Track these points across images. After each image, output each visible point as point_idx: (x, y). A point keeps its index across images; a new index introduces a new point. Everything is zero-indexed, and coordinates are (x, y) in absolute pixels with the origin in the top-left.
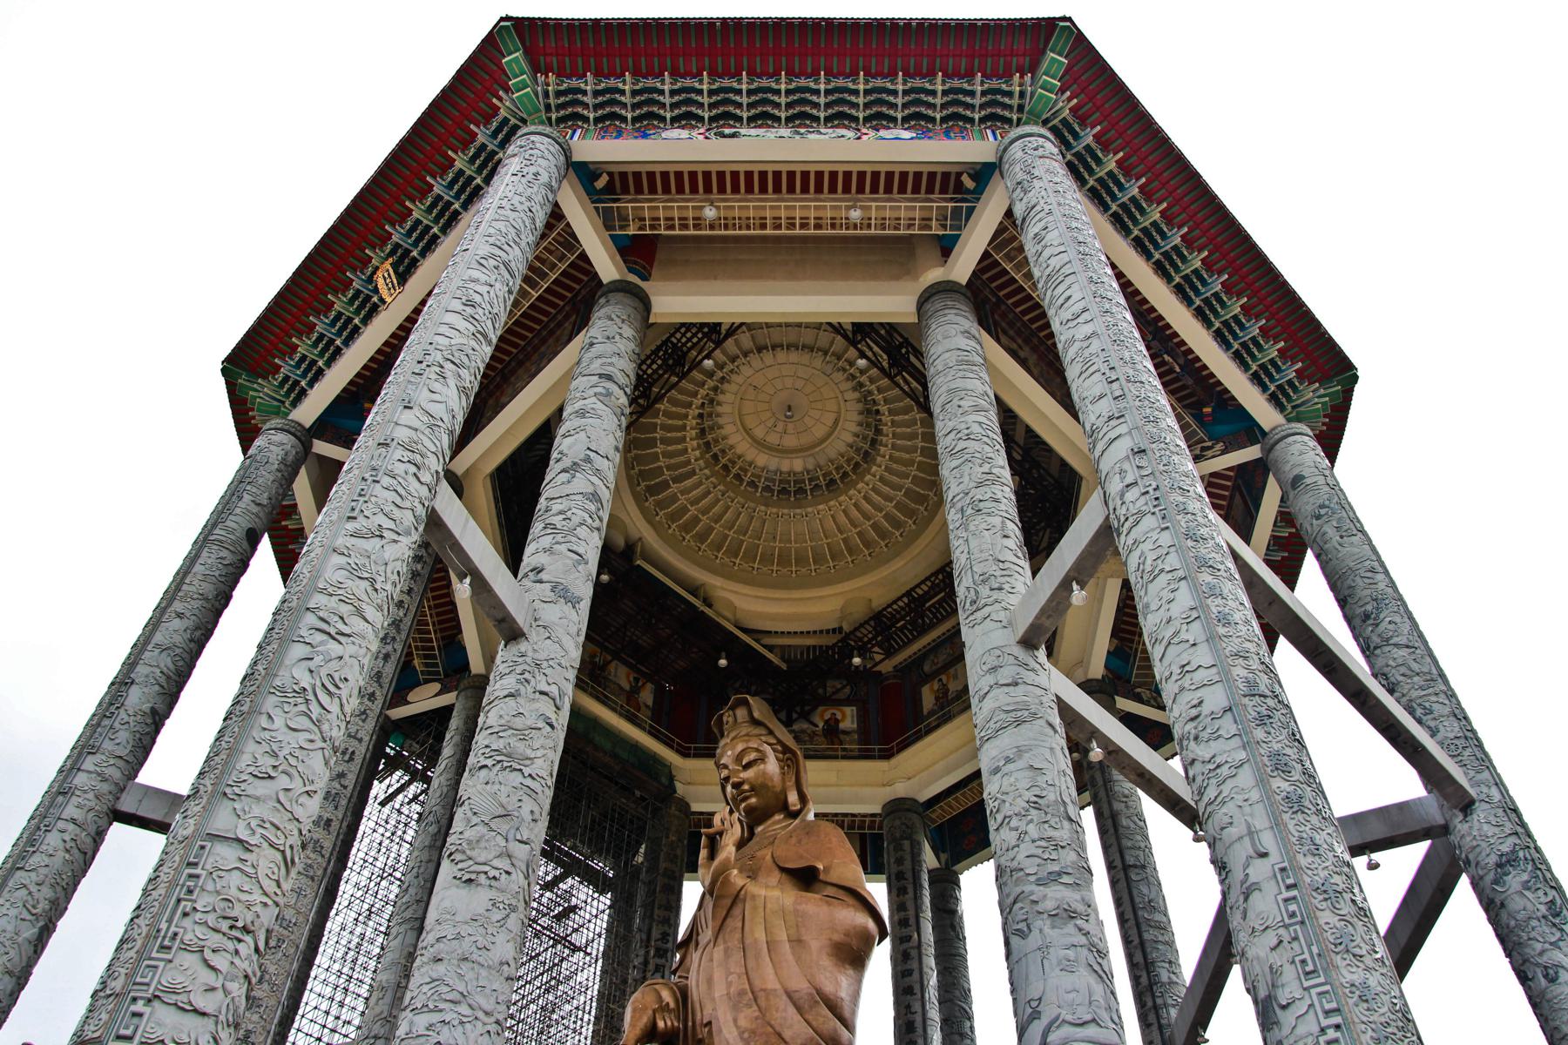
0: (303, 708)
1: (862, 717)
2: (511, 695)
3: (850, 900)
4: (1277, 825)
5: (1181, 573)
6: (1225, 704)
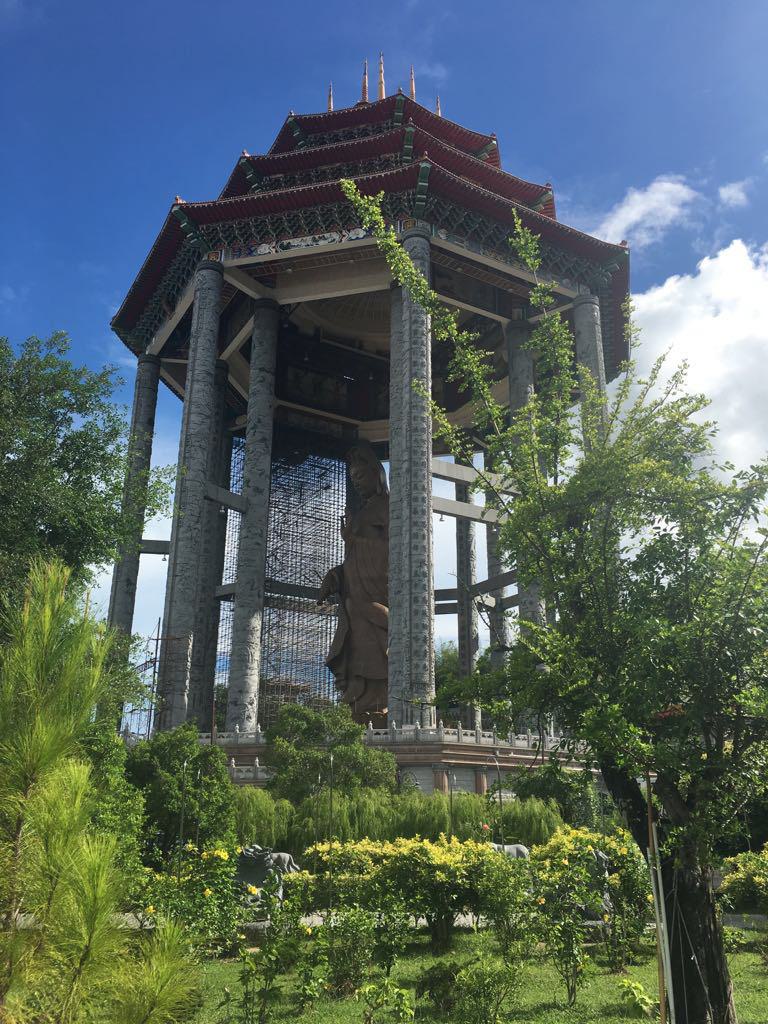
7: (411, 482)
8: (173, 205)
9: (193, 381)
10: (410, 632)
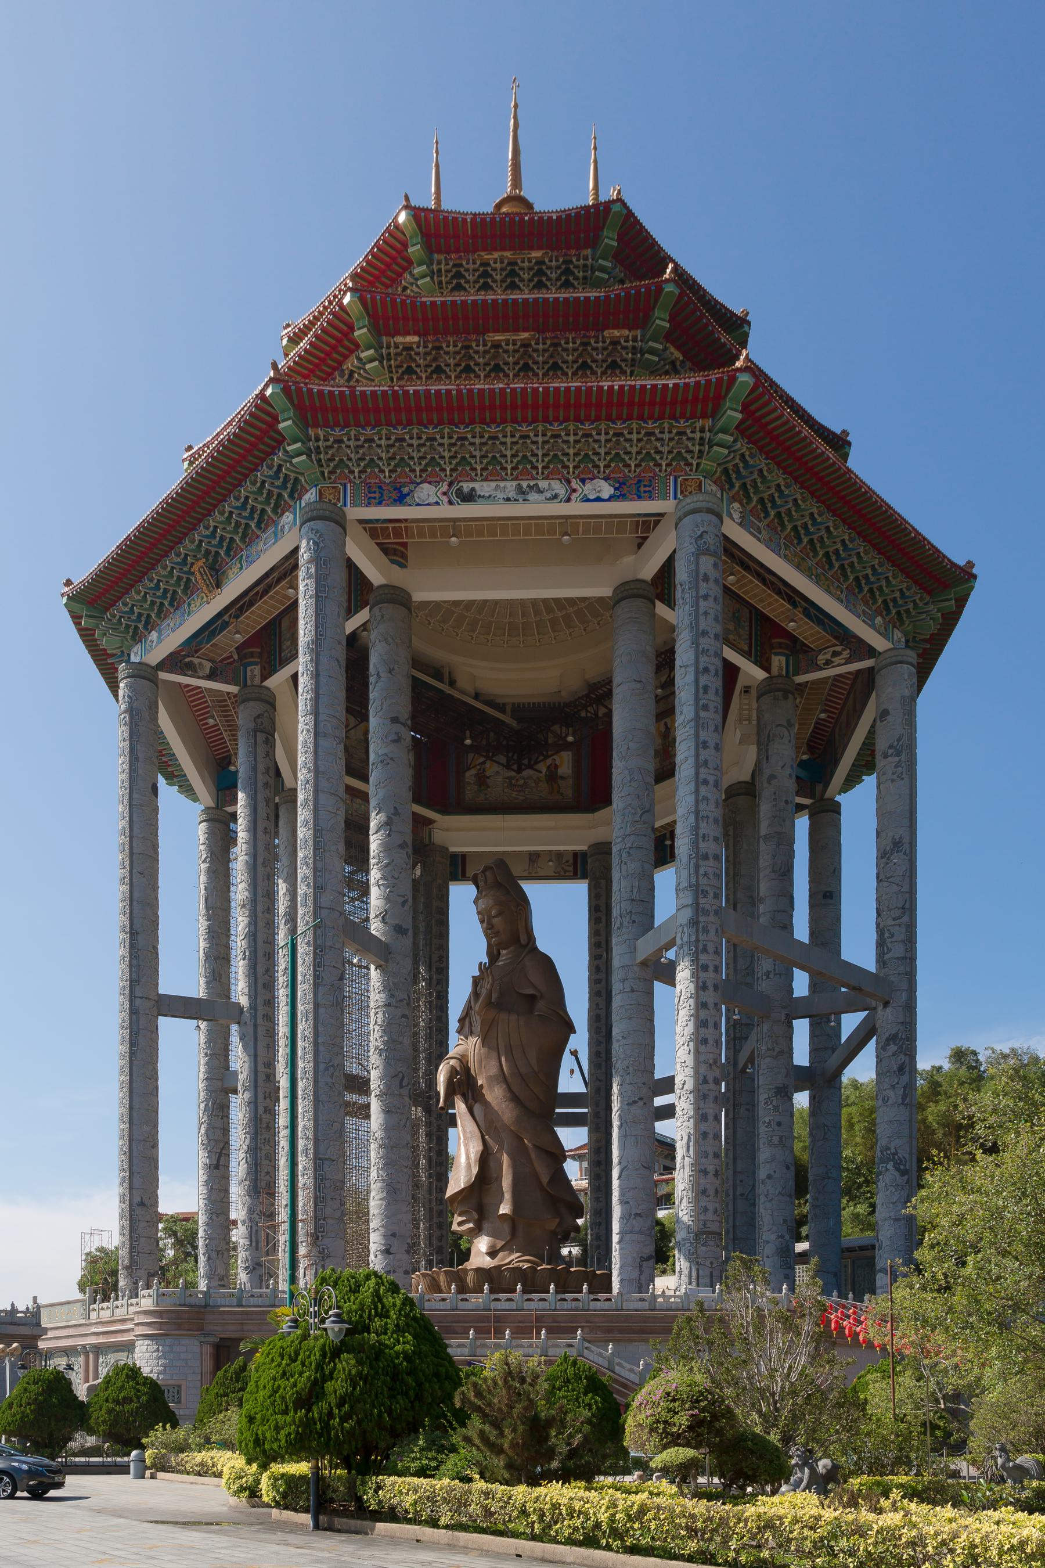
1: (577, 763)
7: (697, 940)
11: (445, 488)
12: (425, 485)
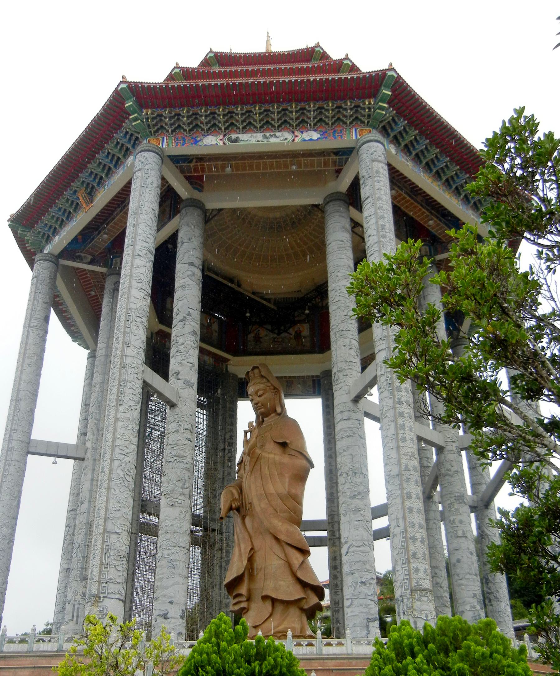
0: (123, 484)
2: (175, 432)
3: (300, 456)
4: (404, 517)
5: (392, 419)
6: (397, 473)
8: (121, 82)
9: (133, 255)
10: (406, 532)
11: (221, 137)
12: (210, 137)
